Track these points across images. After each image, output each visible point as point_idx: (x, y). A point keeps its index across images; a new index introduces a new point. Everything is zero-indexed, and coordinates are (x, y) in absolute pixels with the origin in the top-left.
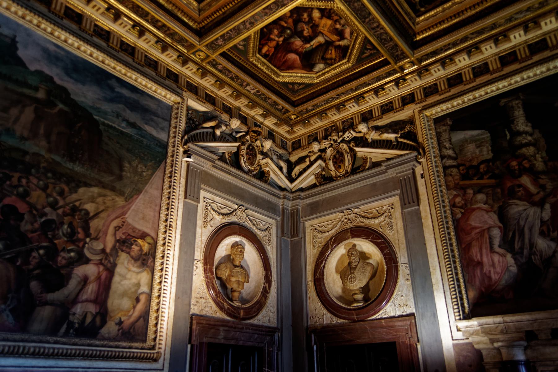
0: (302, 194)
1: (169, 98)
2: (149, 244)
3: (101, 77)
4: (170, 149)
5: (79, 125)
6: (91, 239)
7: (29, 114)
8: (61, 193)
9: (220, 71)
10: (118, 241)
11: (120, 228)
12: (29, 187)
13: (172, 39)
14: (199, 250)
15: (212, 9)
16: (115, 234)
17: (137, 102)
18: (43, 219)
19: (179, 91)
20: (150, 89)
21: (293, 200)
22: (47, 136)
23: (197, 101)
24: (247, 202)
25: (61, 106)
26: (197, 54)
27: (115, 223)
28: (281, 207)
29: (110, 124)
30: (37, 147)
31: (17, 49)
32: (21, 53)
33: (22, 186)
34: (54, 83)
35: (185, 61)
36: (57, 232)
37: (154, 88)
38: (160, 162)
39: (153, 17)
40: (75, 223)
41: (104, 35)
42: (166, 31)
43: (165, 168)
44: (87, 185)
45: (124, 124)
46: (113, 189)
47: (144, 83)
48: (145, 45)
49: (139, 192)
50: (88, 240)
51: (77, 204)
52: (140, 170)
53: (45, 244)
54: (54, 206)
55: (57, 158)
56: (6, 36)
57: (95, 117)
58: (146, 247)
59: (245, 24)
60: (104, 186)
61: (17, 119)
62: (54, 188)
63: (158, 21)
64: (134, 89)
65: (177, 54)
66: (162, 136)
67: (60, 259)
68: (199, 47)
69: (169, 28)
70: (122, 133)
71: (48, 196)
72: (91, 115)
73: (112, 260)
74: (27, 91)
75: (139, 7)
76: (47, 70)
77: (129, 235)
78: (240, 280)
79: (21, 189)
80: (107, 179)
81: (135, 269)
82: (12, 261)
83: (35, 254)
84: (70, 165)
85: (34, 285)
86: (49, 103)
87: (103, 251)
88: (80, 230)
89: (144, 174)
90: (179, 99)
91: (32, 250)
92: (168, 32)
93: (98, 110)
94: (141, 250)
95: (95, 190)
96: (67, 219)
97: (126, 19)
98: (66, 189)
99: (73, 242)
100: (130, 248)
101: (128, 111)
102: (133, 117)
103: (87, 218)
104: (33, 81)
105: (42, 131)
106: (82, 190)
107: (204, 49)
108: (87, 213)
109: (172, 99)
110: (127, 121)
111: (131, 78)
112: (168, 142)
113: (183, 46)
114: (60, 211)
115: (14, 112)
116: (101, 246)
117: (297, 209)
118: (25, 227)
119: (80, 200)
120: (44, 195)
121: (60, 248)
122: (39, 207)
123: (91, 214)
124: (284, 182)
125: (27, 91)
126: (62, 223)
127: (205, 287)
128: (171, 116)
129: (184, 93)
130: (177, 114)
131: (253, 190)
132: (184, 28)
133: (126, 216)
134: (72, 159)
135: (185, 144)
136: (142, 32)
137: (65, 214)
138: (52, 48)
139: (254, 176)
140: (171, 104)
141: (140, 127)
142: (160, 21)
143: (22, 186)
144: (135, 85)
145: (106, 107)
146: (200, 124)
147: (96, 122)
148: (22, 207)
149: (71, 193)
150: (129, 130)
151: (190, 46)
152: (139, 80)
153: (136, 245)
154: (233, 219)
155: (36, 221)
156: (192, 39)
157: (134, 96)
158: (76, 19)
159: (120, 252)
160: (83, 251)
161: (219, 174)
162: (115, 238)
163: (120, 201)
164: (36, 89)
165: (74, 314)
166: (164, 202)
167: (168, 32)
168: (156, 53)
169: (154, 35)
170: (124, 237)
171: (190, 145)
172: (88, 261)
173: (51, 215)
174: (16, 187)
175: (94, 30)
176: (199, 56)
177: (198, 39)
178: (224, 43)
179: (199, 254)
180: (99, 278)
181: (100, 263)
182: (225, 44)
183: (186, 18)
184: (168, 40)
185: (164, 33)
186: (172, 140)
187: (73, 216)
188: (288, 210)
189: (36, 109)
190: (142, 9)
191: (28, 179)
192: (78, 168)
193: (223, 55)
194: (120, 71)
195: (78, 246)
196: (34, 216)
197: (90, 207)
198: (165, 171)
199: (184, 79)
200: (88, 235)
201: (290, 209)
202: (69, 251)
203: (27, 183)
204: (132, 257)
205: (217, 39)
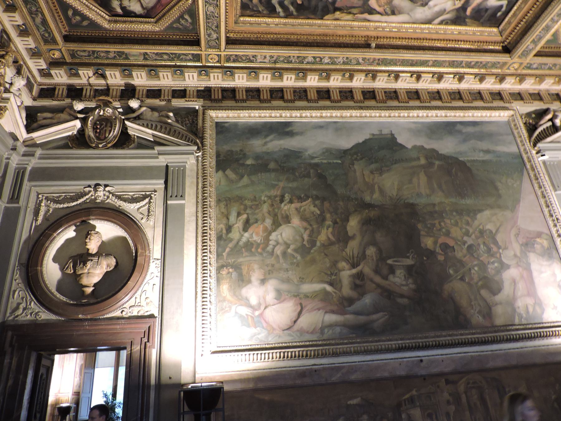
1: (501, 116)
2: (547, 240)
3: (449, 128)
4: (525, 157)
5: (454, 170)
6: (503, 250)
7: (423, 178)
8: (468, 224)
9: (537, 69)
10: (522, 245)
11: (518, 234)
12: (447, 227)
13: (486, 68)
15: (513, 25)
16: (517, 241)
17: (479, 131)
18: (466, 246)
19: (507, 105)
20: (486, 116)
22: (440, 187)
23: (525, 104)
25: (437, 163)
27: (513, 232)
29: (473, 159)
30: (438, 198)
31: (396, 139)
32: (400, 140)
33: (443, 228)
34: (425, 149)
35: (502, 78)
36: (478, 252)
37: (488, 115)
38: (522, 171)
40: (486, 242)
43: (529, 174)
44: (480, 211)
45: (481, 154)
46: (499, 207)
47: (479, 115)
49: (517, 201)
50: (501, 251)
51: (481, 227)
52: (510, 184)
53: (476, 263)
54: (467, 234)
55: (453, 200)
56: (387, 134)
57: (460, 159)
58: (545, 243)
60: (491, 207)
61: (419, 184)
62: (462, 221)
63: (471, 62)
64: (474, 124)
65: (494, 77)
66: (513, 149)
67: (489, 270)
68: (512, 61)
70: (484, 162)
71: (461, 229)
72: (457, 159)
73: (524, 260)
74: (414, 163)
76: (418, 143)
77: (527, 237)
79: (444, 230)
80: (491, 200)
81: (545, 263)
82: (462, 279)
83: (473, 271)
84: (463, 202)
85: (484, 292)
86: (430, 165)
87: (515, 256)
88: (492, 246)
89: (515, 185)
90: (511, 112)
91: (470, 270)
93: (460, 153)
94: (543, 246)
95: (487, 213)
96: (480, 241)
98: (469, 220)
99: (492, 256)
100: (534, 248)
101: (479, 143)
102: (484, 145)
103: (493, 236)
104: (414, 154)
105: (435, 186)
106: (479, 216)
108: (491, 232)
109: (506, 115)
110: (483, 151)
111: (469, 116)
112: (520, 152)
114: (473, 236)
115: (415, 180)
116: (512, 253)
118: (459, 254)
119: (481, 224)
120: (458, 229)
121: (486, 263)
122: (460, 238)
123: (494, 232)
125: (414, 163)
126: (479, 245)
128: (511, 129)
129: (513, 105)
130: (515, 125)
132: (493, 54)
133: (518, 224)
134: (462, 196)
135: (535, 145)
137: (477, 238)
138: (413, 126)
140: (506, 119)
141: (494, 151)
143: (443, 228)
144: (474, 120)
145: (464, 148)
146: (537, 123)
147: (463, 164)
148: (451, 243)
149: (473, 221)
150: (487, 157)
152: (475, 115)
153: (537, 244)
155: (463, 249)
157: (477, 129)
159: (527, 253)
160: (501, 260)
162: (519, 243)
163: (508, 214)
164: (418, 159)
165: (519, 308)
166: (542, 201)
167: (481, 65)
170: (524, 241)
171: (540, 145)
172: (508, 267)
173: (470, 241)
174: (440, 230)
180: (522, 277)
181: (518, 265)
182: (536, 46)
183: (491, 45)
185: (479, 67)
186: (522, 149)
187: (483, 237)
189: (425, 172)
190: (457, 61)
191: (444, 222)
192: (468, 201)
193: (538, 54)
194: (460, 116)
195: (497, 258)
196: (460, 245)
197: (489, 227)
198: (529, 176)
200: (499, 248)
202: (493, 263)
203: (445, 225)
204: (539, 255)
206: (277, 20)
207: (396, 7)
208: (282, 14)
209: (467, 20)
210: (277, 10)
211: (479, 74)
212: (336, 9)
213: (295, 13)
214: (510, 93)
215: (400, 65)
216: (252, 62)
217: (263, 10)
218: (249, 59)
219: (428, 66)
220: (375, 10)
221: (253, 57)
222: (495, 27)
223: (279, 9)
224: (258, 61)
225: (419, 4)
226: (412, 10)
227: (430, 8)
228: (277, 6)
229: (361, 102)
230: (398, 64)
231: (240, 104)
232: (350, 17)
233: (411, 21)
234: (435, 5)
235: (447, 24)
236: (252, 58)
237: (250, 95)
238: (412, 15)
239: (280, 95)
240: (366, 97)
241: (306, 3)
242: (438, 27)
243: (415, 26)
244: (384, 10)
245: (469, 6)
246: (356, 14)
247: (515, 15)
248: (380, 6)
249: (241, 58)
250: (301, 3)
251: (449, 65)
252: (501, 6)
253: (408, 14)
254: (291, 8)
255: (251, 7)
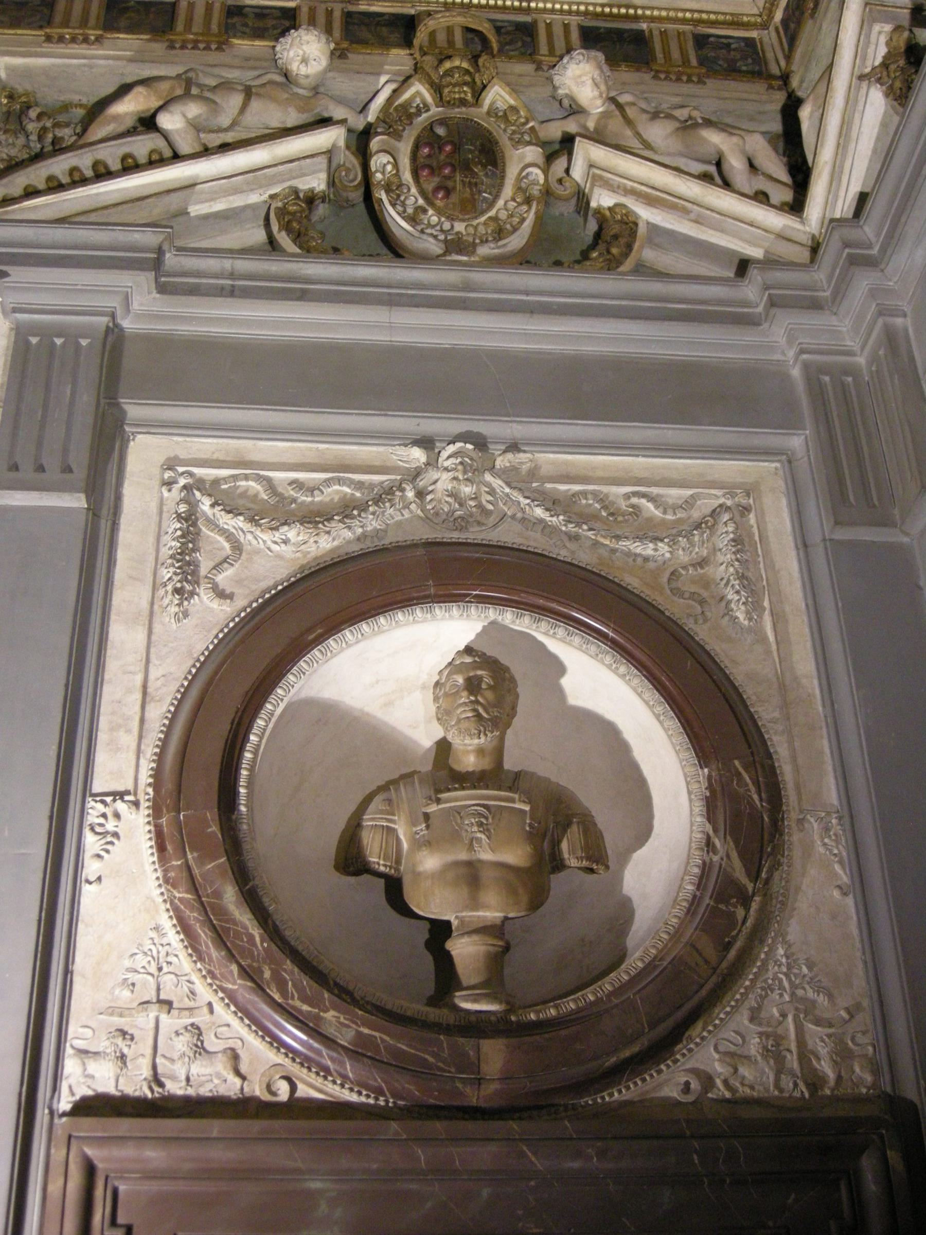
0: (869, 230)
14: (129, 740)
21: (839, 294)
24: (500, 407)
28: (796, 372)
78: (486, 856)
117: (892, 339)
124: (748, 223)
127: (174, 938)
131: (527, 336)
139: (523, 259)
154: (397, 520)
161: (262, 323)
179: (123, 757)
188: (847, 370)
201: (861, 360)
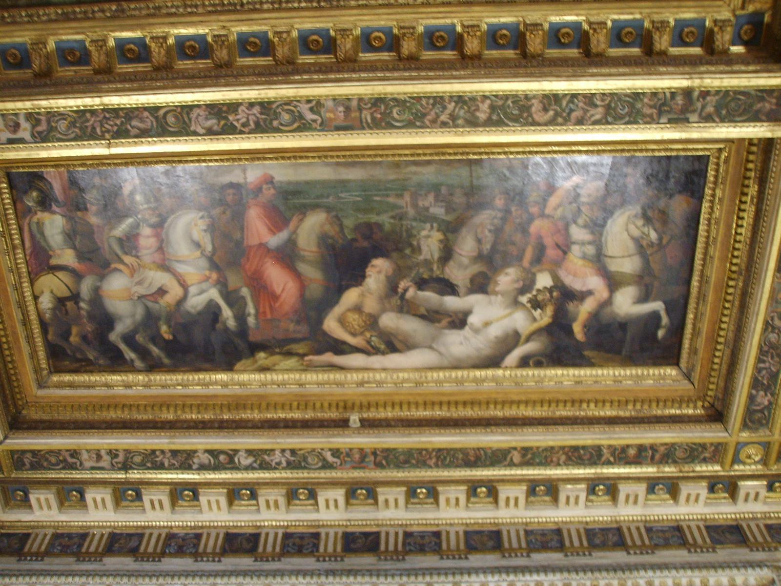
13: (675, 462)
26: (742, 456)
39: (612, 449)
41: (552, 540)
42: (653, 458)
48: (633, 509)
59: (773, 328)
63: (624, 449)
65: (704, 484)
69: (653, 448)
75: (576, 449)
92: (657, 456)
97: (569, 486)
107: (745, 435)
113: (705, 461)
132: (677, 426)
136: (611, 488)
142: (628, 446)
151: (716, 453)
156: (710, 434)
158: (491, 544)
168: (664, 510)
169: (638, 479)
175: (528, 543)
176: (749, 457)
177: (719, 426)
178: (772, 395)
183: (672, 407)
184: (669, 470)
185: (652, 461)
199: (758, 526)
205: (751, 398)
206: (131, 377)
207: (391, 334)
208: (138, 364)
209: (587, 353)
210: (127, 357)
211: (659, 478)
212: (254, 348)
213: (166, 361)
214: (768, 527)
215: (437, 466)
216: (72, 467)
217: (96, 358)
218: (65, 460)
219: (512, 465)
220: (344, 343)
221: (72, 456)
222: (668, 364)
223: (129, 355)
224: (88, 464)
225: (444, 322)
226: (434, 339)
227: (476, 331)
228: (123, 347)
229: (334, 557)
230: (432, 462)
231: (25, 566)
232: (292, 362)
233: (446, 363)
234: (487, 324)
235: (539, 364)
236: (70, 460)
237: (60, 545)
238: (442, 349)
239: (133, 543)
240: (352, 546)
241: (182, 338)
242: (520, 372)
243: (460, 373)
244: (369, 342)
245: (575, 319)
246: (305, 355)
247: (696, 333)
248: (354, 335)
249: (47, 460)
250: (171, 337)
251: (569, 458)
252: (654, 317)
253: (430, 347)
254: (155, 350)
255: (69, 352)
